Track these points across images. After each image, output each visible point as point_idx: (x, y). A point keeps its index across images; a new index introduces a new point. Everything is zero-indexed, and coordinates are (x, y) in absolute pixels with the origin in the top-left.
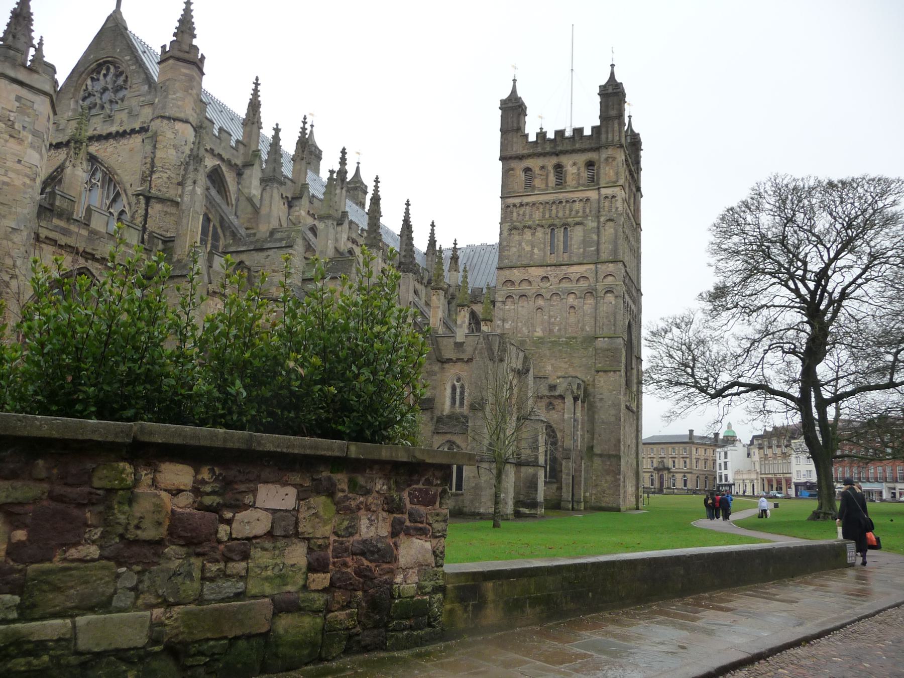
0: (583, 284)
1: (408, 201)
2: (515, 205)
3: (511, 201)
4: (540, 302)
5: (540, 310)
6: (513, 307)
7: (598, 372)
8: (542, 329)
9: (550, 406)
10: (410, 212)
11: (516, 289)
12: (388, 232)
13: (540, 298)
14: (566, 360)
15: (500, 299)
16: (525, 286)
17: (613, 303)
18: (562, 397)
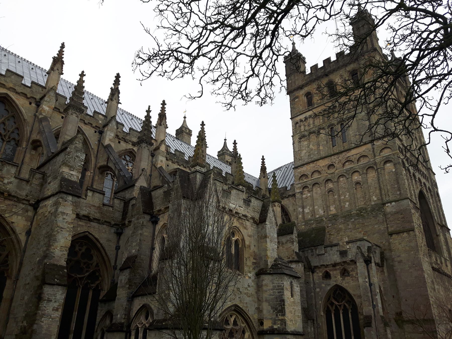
0: (363, 161)
1: (203, 122)
2: (301, 121)
3: (298, 119)
4: (330, 185)
5: (330, 193)
6: (309, 195)
7: (391, 234)
8: (335, 208)
9: (345, 273)
10: (205, 130)
11: (308, 181)
12: (93, 97)
13: (329, 182)
14: (360, 229)
15: (298, 191)
16: (316, 176)
17: (394, 170)
18: (354, 262)
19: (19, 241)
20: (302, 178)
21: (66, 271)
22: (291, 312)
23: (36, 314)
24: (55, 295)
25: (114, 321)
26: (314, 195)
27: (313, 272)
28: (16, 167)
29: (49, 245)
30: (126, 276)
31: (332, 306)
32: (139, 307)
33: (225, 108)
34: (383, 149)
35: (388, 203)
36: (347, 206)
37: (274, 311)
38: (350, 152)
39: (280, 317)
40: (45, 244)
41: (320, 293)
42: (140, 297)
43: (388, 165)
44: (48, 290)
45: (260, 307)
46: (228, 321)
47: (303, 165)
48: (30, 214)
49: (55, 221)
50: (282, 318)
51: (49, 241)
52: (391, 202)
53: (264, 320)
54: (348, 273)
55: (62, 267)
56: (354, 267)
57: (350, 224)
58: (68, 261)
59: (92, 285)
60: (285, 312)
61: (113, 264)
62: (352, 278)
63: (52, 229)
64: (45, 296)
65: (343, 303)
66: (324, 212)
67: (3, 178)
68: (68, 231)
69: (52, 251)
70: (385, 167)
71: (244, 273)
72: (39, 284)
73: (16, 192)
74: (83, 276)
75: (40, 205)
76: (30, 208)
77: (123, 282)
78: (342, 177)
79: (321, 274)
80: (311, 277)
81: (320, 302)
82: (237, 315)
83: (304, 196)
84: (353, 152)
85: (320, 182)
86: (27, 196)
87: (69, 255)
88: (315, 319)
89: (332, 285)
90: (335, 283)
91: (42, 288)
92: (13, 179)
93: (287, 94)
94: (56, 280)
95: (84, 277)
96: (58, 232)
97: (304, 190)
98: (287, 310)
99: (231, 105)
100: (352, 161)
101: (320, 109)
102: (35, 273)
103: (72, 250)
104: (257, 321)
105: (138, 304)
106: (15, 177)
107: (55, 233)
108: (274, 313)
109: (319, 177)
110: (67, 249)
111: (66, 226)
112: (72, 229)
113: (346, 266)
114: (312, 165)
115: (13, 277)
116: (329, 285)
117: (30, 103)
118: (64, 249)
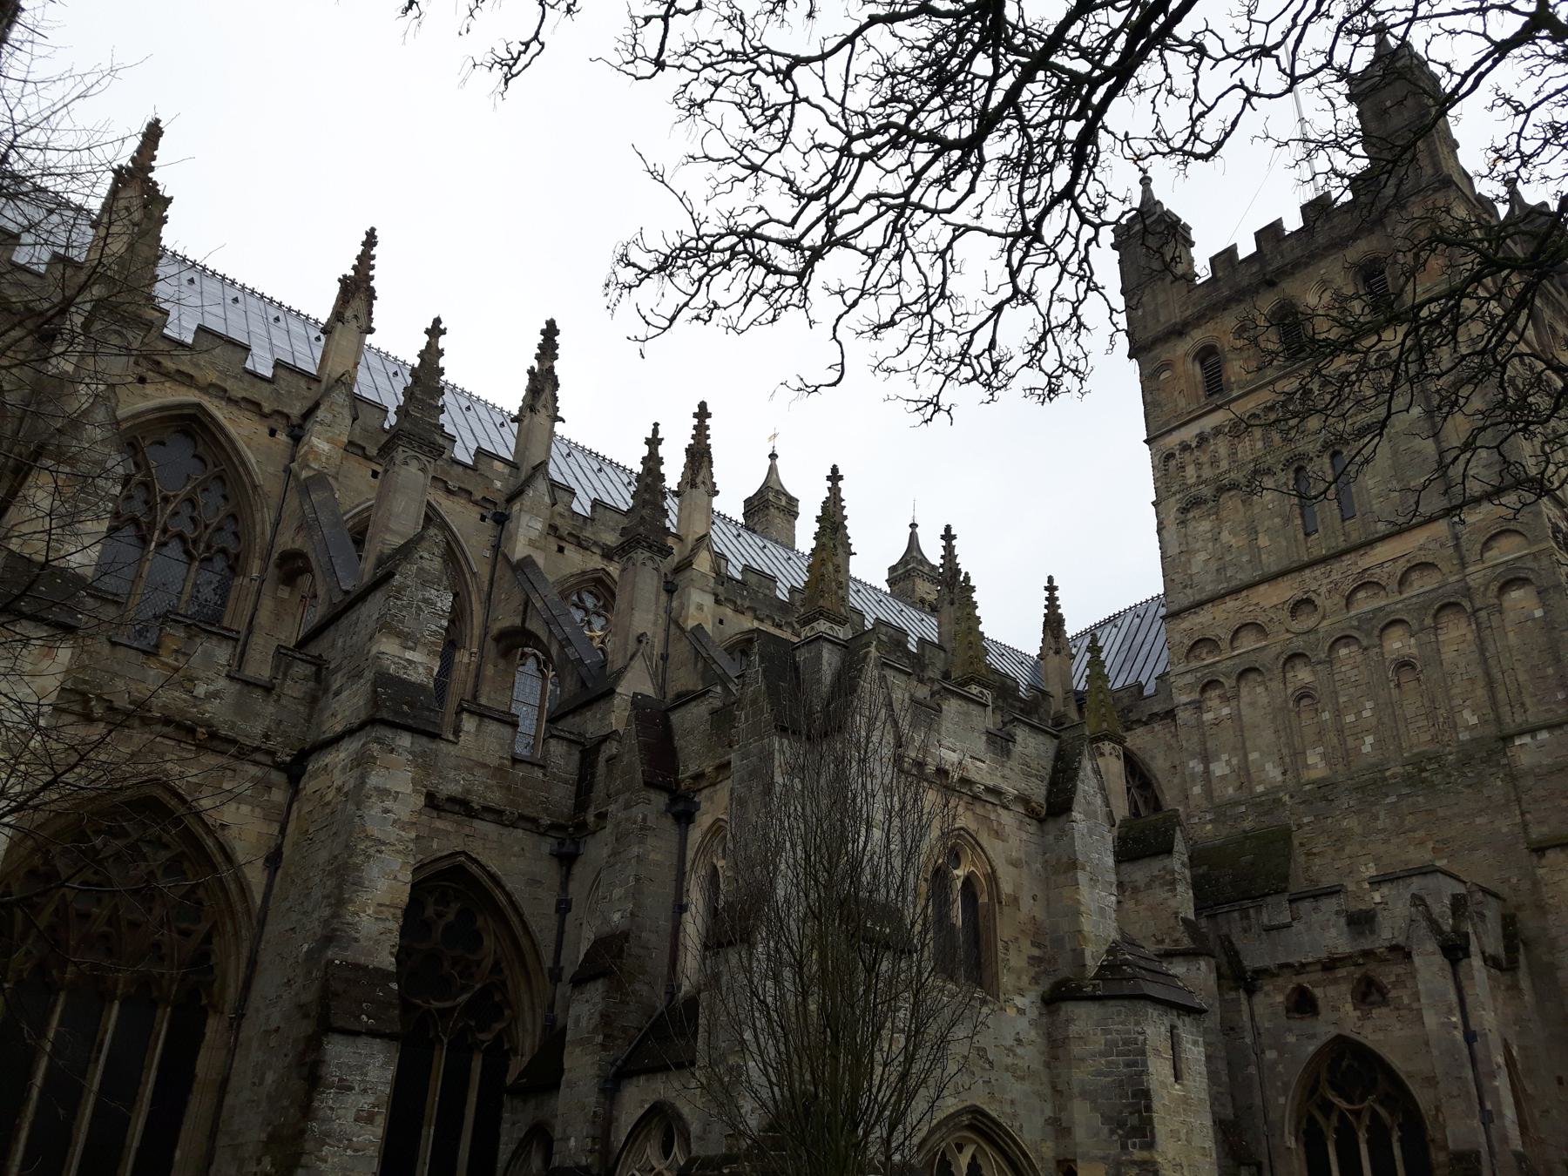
0: (1421, 584)
1: (835, 469)
2: (1185, 447)
3: (1173, 440)
4: (1303, 675)
5: (1304, 702)
6: (1226, 711)
8: (1324, 756)
9: (1369, 993)
10: (843, 495)
11: (1223, 662)
12: (472, 403)
13: (1299, 663)
14: (1420, 834)
15: (1184, 699)
16: (1248, 642)
17: (1538, 613)
18: (1401, 953)
19: (244, 889)
20: (1197, 652)
21: (395, 986)
22: (1174, 1134)
23: (303, 1132)
24: (362, 1069)
25: (556, 1161)
26: (1245, 711)
27: (1251, 992)
28: (231, 643)
29: (339, 902)
30: (594, 1005)
31: (1327, 1117)
32: (641, 1112)
33: (918, 418)
34: (1493, 537)
35: (1521, 734)
36: (1366, 749)
37: (1112, 1132)
38: (1372, 553)
39: (1138, 1155)
40: (328, 897)
41: (1280, 1068)
42: (642, 1079)
43: (1515, 594)
44: (339, 1053)
45: (1063, 1116)
46: (950, 1164)
47: (1200, 604)
48: (278, 796)
49: (357, 819)
50: (1145, 1155)
51: (339, 887)
52: (1533, 731)
53: (1079, 1162)
54: (1382, 992)
55: (382, 975)
56: (1401, 971)
57: (1382, 815)
58: (402, 955)
59: (482, 1036)
60: (1153, 1136)
61: (548, 963)
62: (1396, 1013)
63: (347, 846)
64: (332, 1073)
65: (1366, 1104)
66: (1284, 773)
67: (191, 680)
68: (399, 852)
69: (349, 919)
70: (1505, 605)
71: (1002, 997)
72: (310, 1031)
73: (233, 726)
74: (448, 1004)
75: (310, 767)
76: (277, 777)
77: (584, 1023)
78: (1347, 645)
79: (1280, 998)
80: (1245, 1007)
81: (1282, 1100)
82: (979, 1145)
83: (1208, 717)
84: (1383, 552)
85: (1264, 666)
86: (267, 737)
87: (403, 932)
88: (1266, 1161)
89: (1324, 1039)
90: (1334, 1031)
91: (321, 1044)
92: (222, 683)
93: (1130, 356)
94: (364, 1018)
95: (453, 1009)
96: (369, 857)
97: (1207, 695)
98: (1161, 1131)
99: (938, 408)
100: (1377, 583)
101: (1252, 404)
102: (297, 994)
103: (414, 917)
104: (1052, 1165)
105: (635, 1100)
106: (228, 676)
107: (358, 860)
108: (1115, 1137)
109: (1258, 645)
110: (399, 913)
111: (392, 833)
112: (411, 846)
113: (1373, 968)
114: (1231, 604)
115: (227, 1008)
116: (1313, 1036)
117: (273, 433)
118: (387, 913)
